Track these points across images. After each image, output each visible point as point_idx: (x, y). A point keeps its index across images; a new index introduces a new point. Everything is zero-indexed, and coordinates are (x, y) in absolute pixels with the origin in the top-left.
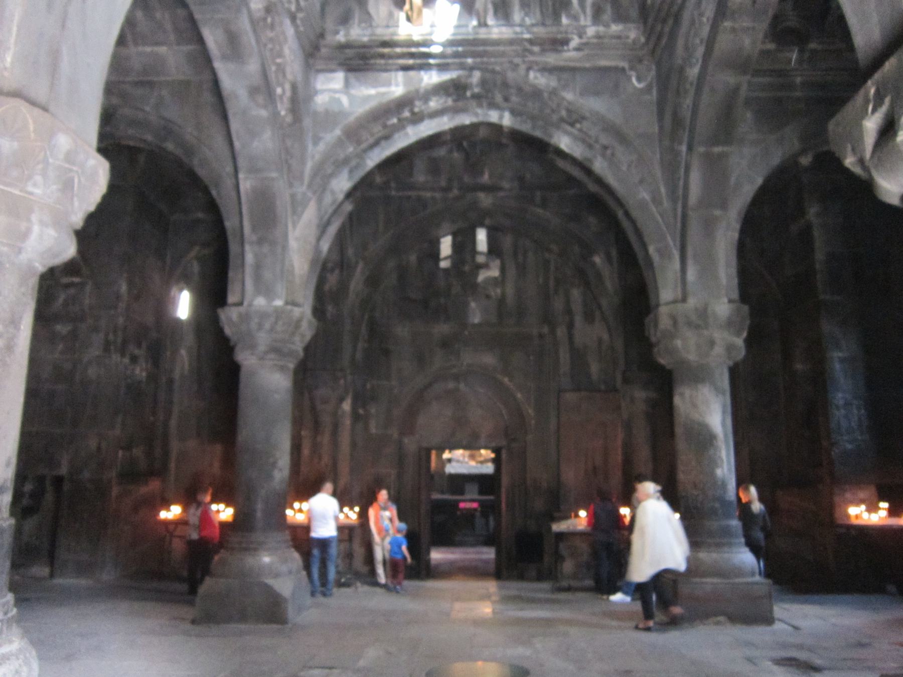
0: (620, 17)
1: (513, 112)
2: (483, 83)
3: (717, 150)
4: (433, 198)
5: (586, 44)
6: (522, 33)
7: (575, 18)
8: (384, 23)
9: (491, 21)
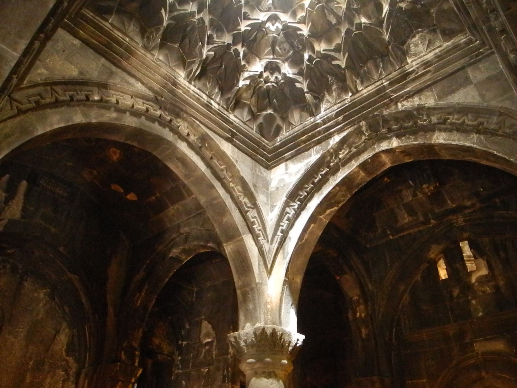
0: (448, 34)
1: (398, 136)
2: (370, 127)
4: (420, 231)
6: (382, 83)
8: (299, 124)
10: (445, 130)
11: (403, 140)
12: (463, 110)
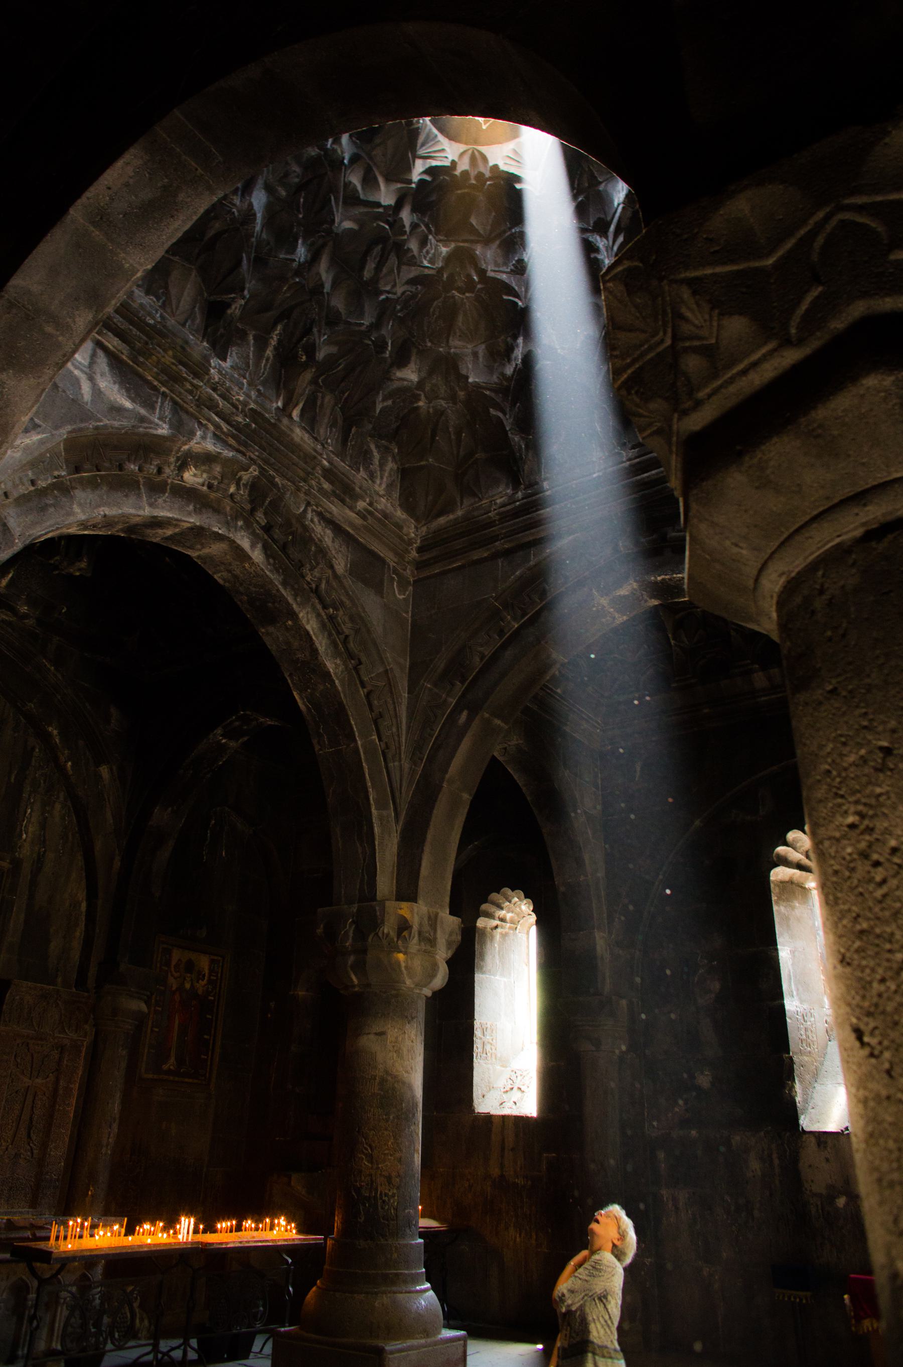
0: (408, 505)
1: (265, 548)
2: (254, 486)
3: (498, 722)
5: (370, 513)
7: (372, 476)
9: (296, 414)
10: (318, 615)
11: (269, 564)
12: (359, 620)
